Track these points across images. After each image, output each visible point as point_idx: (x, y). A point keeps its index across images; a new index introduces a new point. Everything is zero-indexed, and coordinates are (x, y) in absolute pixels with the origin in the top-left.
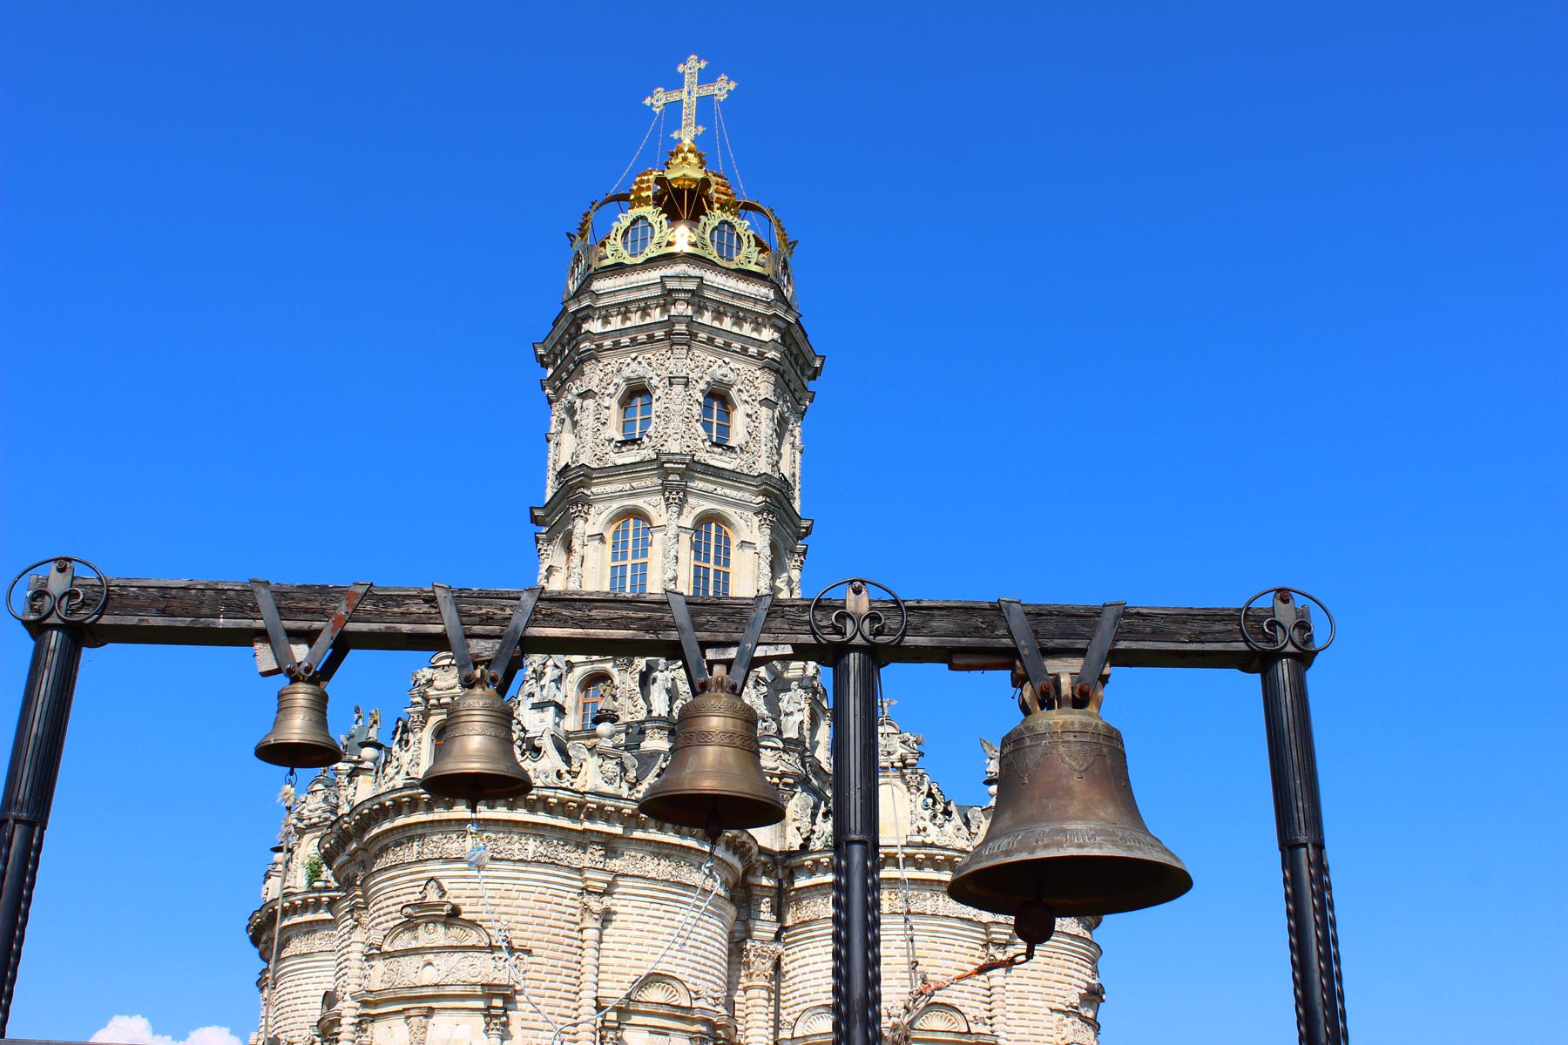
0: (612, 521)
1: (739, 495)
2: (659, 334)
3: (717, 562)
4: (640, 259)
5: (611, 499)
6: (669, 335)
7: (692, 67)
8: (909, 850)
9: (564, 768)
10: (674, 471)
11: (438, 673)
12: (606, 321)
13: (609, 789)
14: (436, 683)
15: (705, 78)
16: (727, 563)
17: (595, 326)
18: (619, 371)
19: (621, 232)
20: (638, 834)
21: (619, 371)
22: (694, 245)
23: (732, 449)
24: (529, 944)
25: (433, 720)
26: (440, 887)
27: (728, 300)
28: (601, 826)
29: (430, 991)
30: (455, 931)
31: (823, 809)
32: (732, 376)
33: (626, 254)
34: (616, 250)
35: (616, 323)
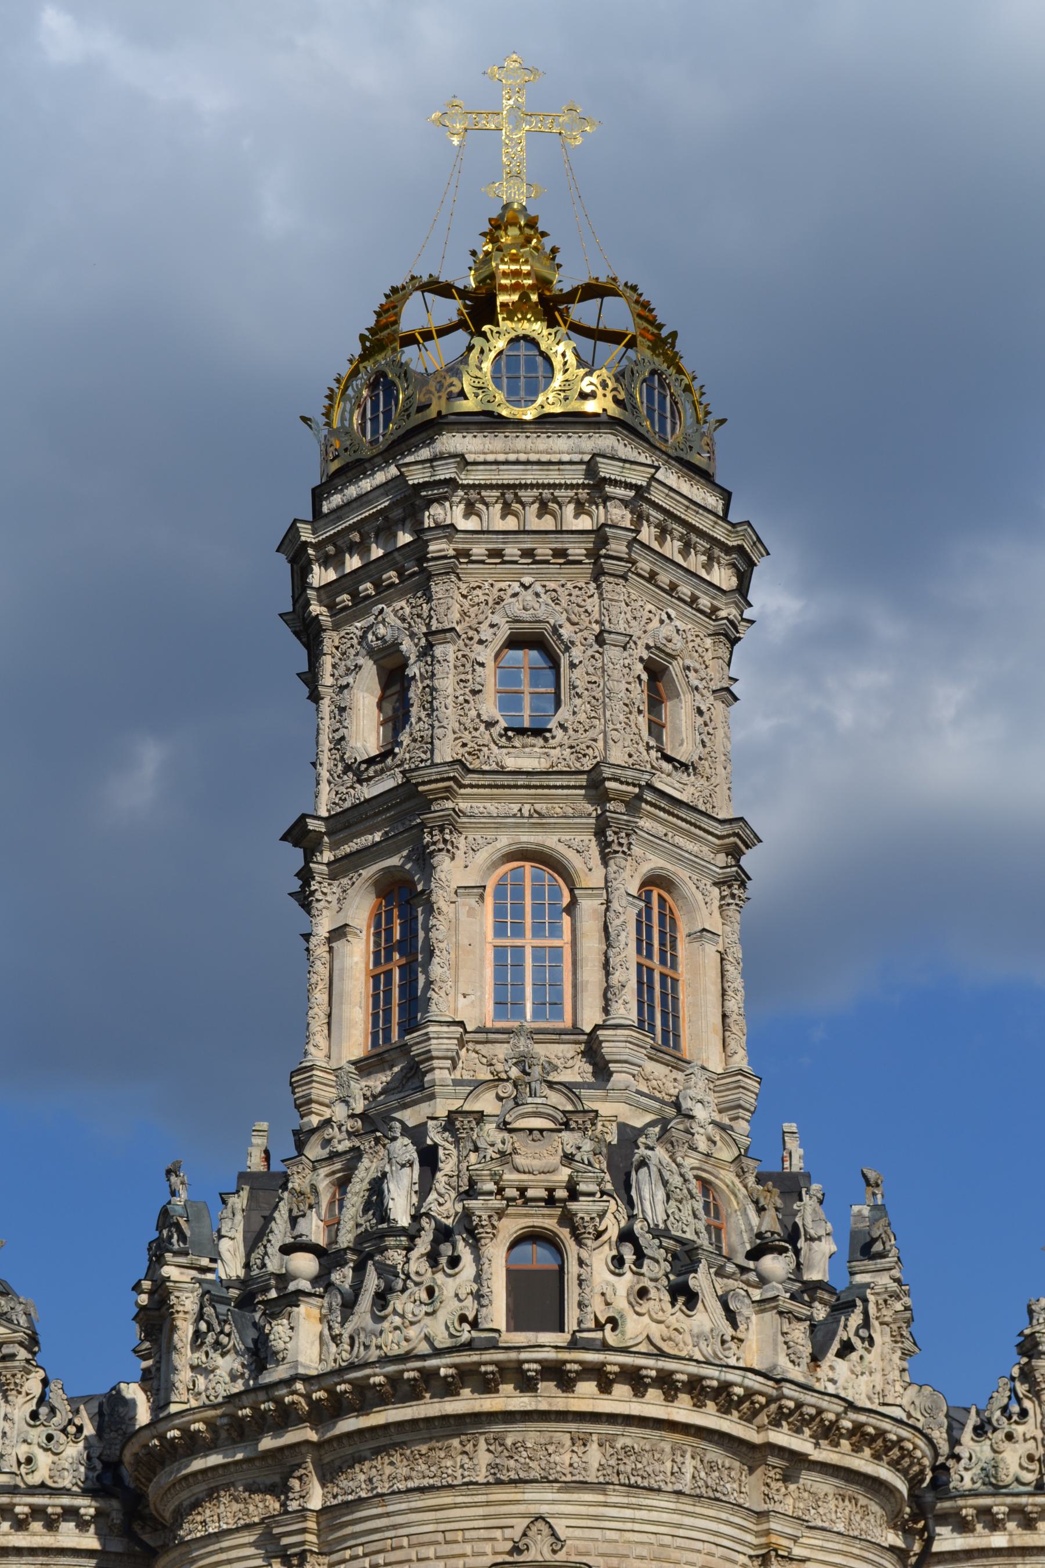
0: (495, 865)
2: (577, 551)
3: (663, 961)
4: (529, 414)
5: (499, 827)
6: (594, 554)
9: (729, 1331)
10: (619, 797)
11: (518, 1141)
12: (470, 510)
13: (796, 1373)
14: (518, 1160)
16: (674, 966)
17: (455, 515)
18: (499, 601)
19: (492, 355)
21: (499, 601)
26: (554, 1534)
27: (679, 511)
31: (973, 1420)
32: (678, 643)
33: (500, 397)
35: (495, 519)
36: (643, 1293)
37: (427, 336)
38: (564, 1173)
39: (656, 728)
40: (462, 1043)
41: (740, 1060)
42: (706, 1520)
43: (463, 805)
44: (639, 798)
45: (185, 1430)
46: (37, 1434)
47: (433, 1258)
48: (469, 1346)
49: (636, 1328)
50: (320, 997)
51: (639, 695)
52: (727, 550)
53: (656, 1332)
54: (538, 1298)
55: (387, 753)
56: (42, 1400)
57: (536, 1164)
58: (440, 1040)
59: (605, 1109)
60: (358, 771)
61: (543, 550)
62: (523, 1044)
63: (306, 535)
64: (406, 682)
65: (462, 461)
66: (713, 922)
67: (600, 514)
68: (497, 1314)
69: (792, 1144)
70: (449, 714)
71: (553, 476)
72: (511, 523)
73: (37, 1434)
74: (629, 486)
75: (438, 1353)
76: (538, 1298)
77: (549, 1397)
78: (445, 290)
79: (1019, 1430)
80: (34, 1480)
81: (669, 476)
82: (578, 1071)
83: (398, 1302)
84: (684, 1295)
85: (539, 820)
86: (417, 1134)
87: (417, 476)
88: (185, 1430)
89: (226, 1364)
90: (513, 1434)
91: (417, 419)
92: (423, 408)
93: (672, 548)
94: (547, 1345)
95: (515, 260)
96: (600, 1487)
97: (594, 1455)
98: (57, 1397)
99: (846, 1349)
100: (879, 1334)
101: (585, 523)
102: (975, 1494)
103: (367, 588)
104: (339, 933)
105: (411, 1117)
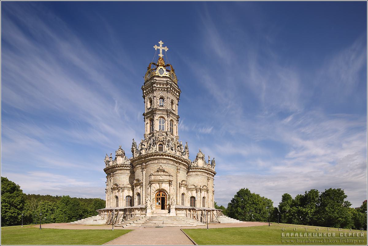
6: (167, 90)
12: (157, 85)
15: (163, 46)
20: (182, 163)
24: (173, 175)
28: (179, 161)
29: (162, 180)
35: (159, 86)
43: (156, 112)
55: (151, 108)
58: (155, 132)
60: (148, 109)
65: (156, 80)
67: (168, 86)
70: (155, 104)
74: (170, 84)
86: (153, 139)
96: (165, 164)
97: (165, 161)
99: (184, 155)
104: (147, 123)
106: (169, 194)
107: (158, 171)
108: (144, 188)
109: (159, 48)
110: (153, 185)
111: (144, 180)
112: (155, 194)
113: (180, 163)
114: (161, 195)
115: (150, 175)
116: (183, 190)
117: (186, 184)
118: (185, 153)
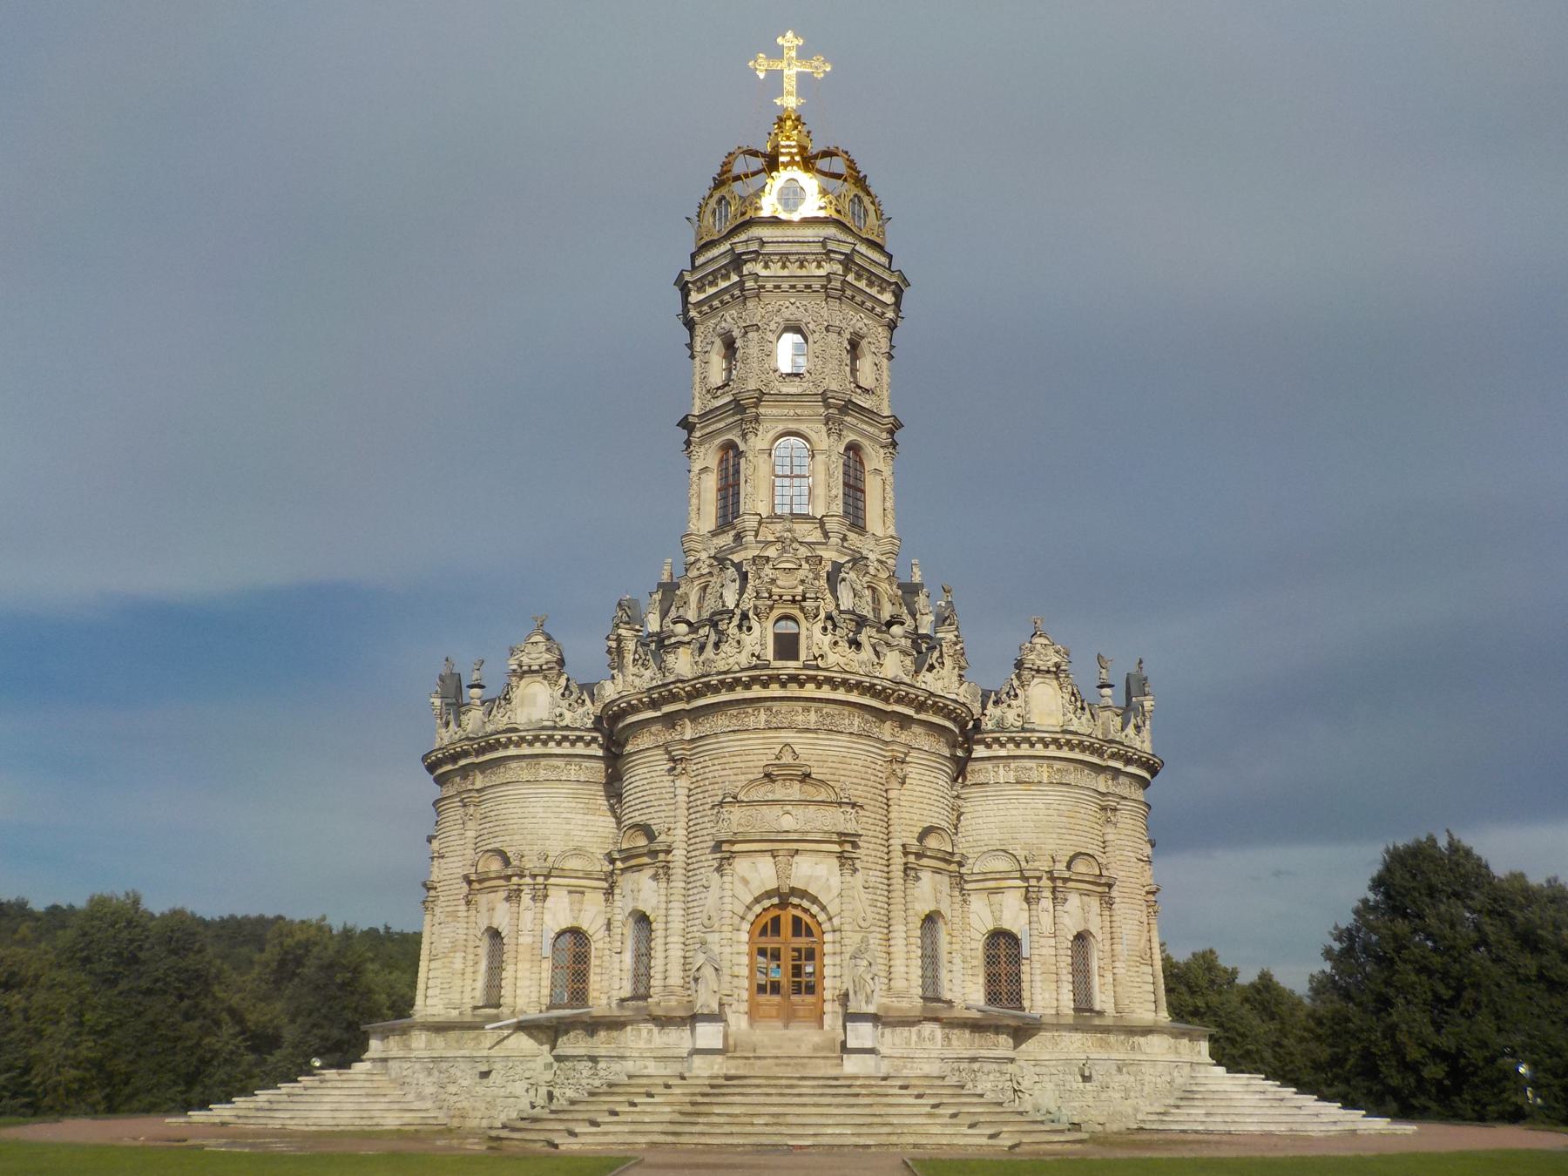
1: (871, 430)
2: (816, 286)
4: (796, 217)
7: (789, 41)
8: (1069, 737)
10: (835, 406)
12: (766, 266)
13: (907, 680)
15: (803, 54)
17: (758, 268)
20: (923, 716)
22: (838, 212)
23: (867, 391)
24: (860, 801)
25: (776, 613)
27: (867, 266)
30: (806, 787)
33: (780, 208)
34: (769, 205)
36: (836, 643)
37: (747, 176)
38: (800, 589)
39: (854, 371)
40: (760, 523)
41: (891, 531)
42: (863, 744)
43: (761, 410)
44: (845, 406)
45: (629, 703)
46: (565, 703)
47: (740, 627)
48: (755, 667)
49: (832, 658)
50: (694, 501)
51: (847, 359)
52: (890, 284)
53: (842, 661)
54: (787, 646)
56: (567, 687)
57: (786, 584)
59: (826, 554)
60: (714, 392)
61: (800, 286)
62: (788, 525)
63: (688, 278)
64: (735, 351)
65: (763, 243)
66: (881, 466)
68: (769, 654)
69: (915, 569)
71: (805, 249)
72: (785, 273)
73: (565, 703)
75: (742, 670)
76: (787, 646)
77: (793, 690)
78: (755, 154)
79: (1014, 703)
80: (564, 724)
81: (862, 248)
82: (817, 536)
83: (724, 647)
84: (856, 644)
85: (798, 418)
86: (738, 566)
87: (740, 249)
88: (629, 703)
89: (648, 674)
90: (776, 706)
91: (740, 220)
92: (743, 214)
93: (862, 284)
94: (791, 667)
95: (788, 138)
96: (815, 731)
97: (813, 717)
98: (574, 687)
99: (931, 668)
100: (948, 661)
101: (822, 272)
102: (992, 731)
103: (716, 303)
105: (736, 558)
106: (836, 921)
107: (767, 775)
108: (678, 884)
109: (778, 65)
110: (741, 866)
111: (680, 832)
112: (746, 926)
113: (904, 722)
114: (786, 927)
115: (721, 804)
116: (929, 891)
117: (952, 854)
118: (936, 654)
